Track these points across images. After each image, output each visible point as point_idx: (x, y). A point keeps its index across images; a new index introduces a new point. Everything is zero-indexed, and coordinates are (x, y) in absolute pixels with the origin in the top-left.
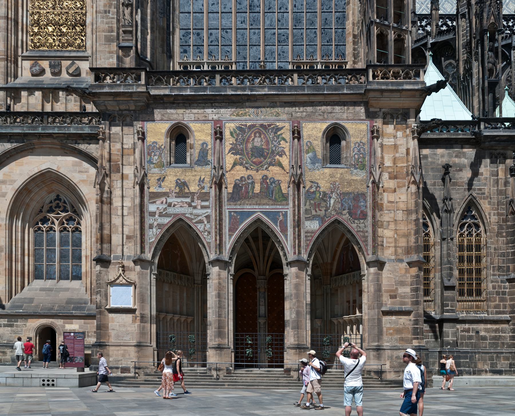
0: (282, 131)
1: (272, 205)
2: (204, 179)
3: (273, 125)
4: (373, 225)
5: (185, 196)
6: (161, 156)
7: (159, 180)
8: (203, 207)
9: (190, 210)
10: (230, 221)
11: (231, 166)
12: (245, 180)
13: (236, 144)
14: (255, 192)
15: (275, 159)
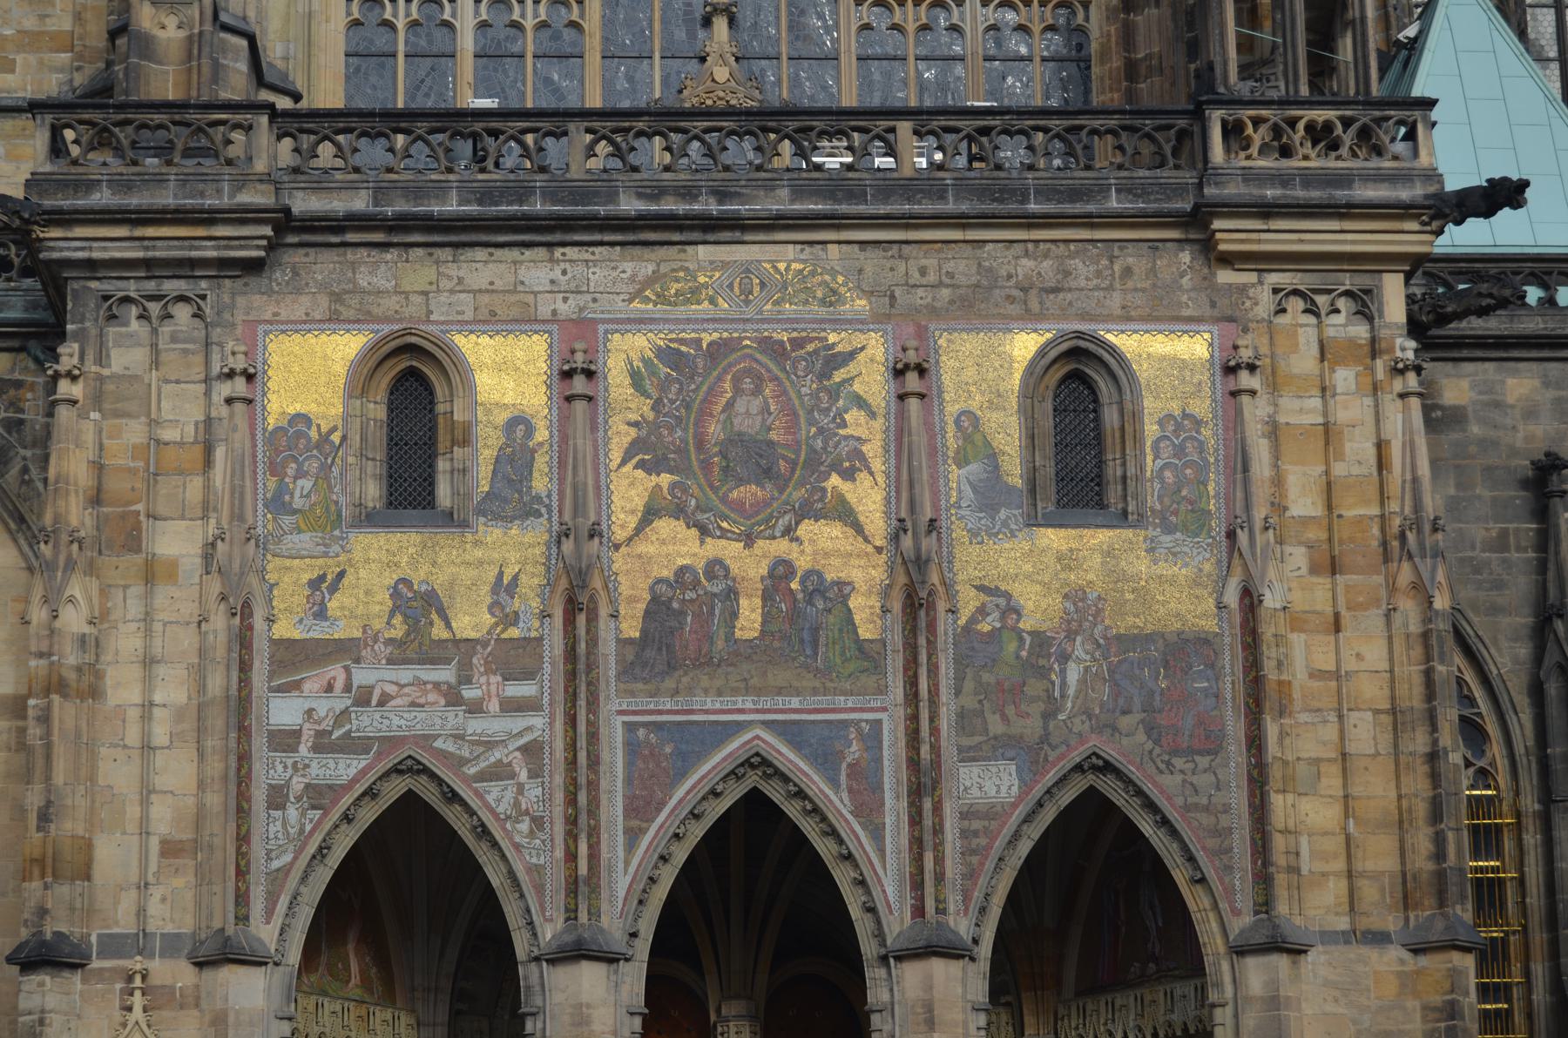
0: (852, 368)
1: (815, 692)
2: (516, 578)
3: (812, 340)
4: (1251, 780)
5: (433, 654)
6: (327, 479)
7: (315, 584)
8: (513, 707)
9: (455, 718)
10: (629, 764)
11: (633, 522)
12: (696, 584)
13: (655, 427)
14: (738, 634)
15: (824, 490)
